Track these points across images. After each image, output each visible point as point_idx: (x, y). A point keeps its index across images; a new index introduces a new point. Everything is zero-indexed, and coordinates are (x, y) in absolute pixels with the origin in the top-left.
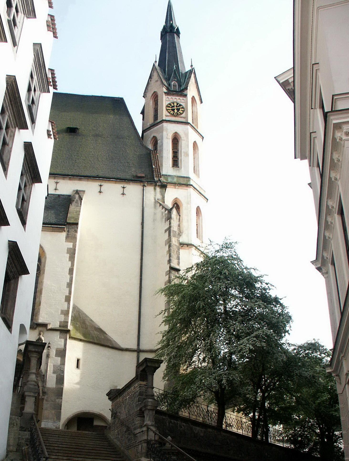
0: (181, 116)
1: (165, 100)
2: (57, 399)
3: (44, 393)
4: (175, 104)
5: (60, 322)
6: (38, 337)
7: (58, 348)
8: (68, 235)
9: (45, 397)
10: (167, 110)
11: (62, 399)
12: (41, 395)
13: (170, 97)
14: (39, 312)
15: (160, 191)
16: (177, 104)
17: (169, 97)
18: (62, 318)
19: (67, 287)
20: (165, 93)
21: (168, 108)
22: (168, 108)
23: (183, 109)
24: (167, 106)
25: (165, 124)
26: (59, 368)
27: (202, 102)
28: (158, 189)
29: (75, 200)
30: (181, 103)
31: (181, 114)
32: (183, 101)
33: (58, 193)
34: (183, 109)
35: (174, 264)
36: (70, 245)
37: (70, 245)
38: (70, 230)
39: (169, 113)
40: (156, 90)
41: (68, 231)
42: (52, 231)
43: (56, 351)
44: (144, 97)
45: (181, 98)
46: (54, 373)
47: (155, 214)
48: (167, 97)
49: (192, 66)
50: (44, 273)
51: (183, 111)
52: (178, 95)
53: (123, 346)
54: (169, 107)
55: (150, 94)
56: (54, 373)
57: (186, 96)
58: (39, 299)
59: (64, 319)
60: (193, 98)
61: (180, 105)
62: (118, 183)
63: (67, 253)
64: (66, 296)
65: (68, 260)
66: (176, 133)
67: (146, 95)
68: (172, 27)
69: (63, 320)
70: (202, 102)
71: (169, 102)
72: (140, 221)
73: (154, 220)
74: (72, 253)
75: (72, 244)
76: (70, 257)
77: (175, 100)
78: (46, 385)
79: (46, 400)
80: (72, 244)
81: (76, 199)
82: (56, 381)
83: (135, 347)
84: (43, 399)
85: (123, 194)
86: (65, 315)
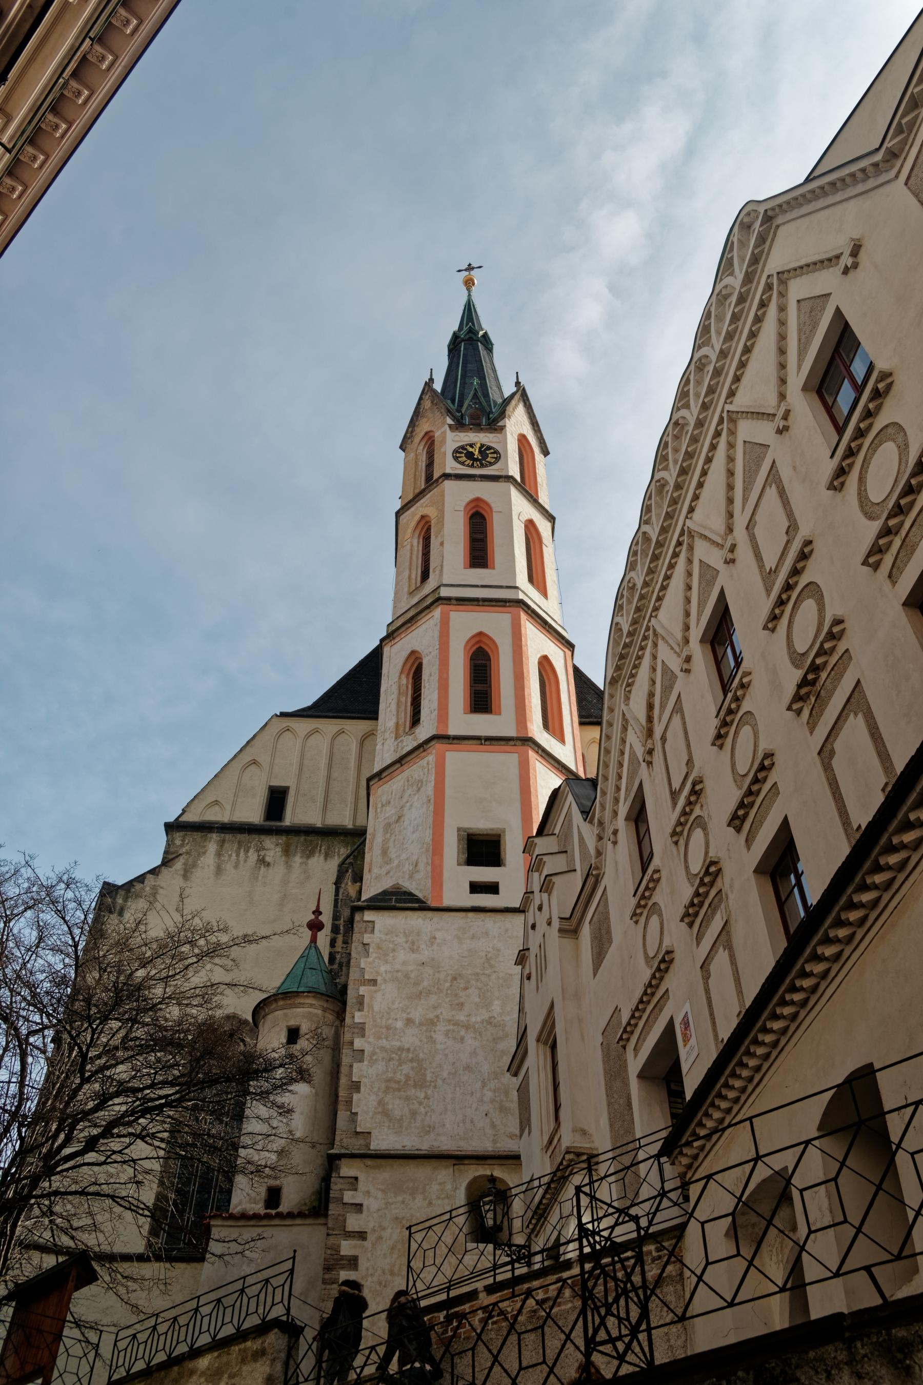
1: (451, 440)
10: (456, 459)
13: (462, 435)
20: (450, 426)
24: (456, 451)
25: (448, 484)
27: (546, 452)
31: (491, 464)
34: (495, 455)
39: (463, 463)
44: (401, 447)
51: (498, 459)
54: (461, 453)
57: (503, 428)
60: (522, 439)
61: (489, 448)
66: (478, 500)
68: (472, 332)
70: (546, 452)
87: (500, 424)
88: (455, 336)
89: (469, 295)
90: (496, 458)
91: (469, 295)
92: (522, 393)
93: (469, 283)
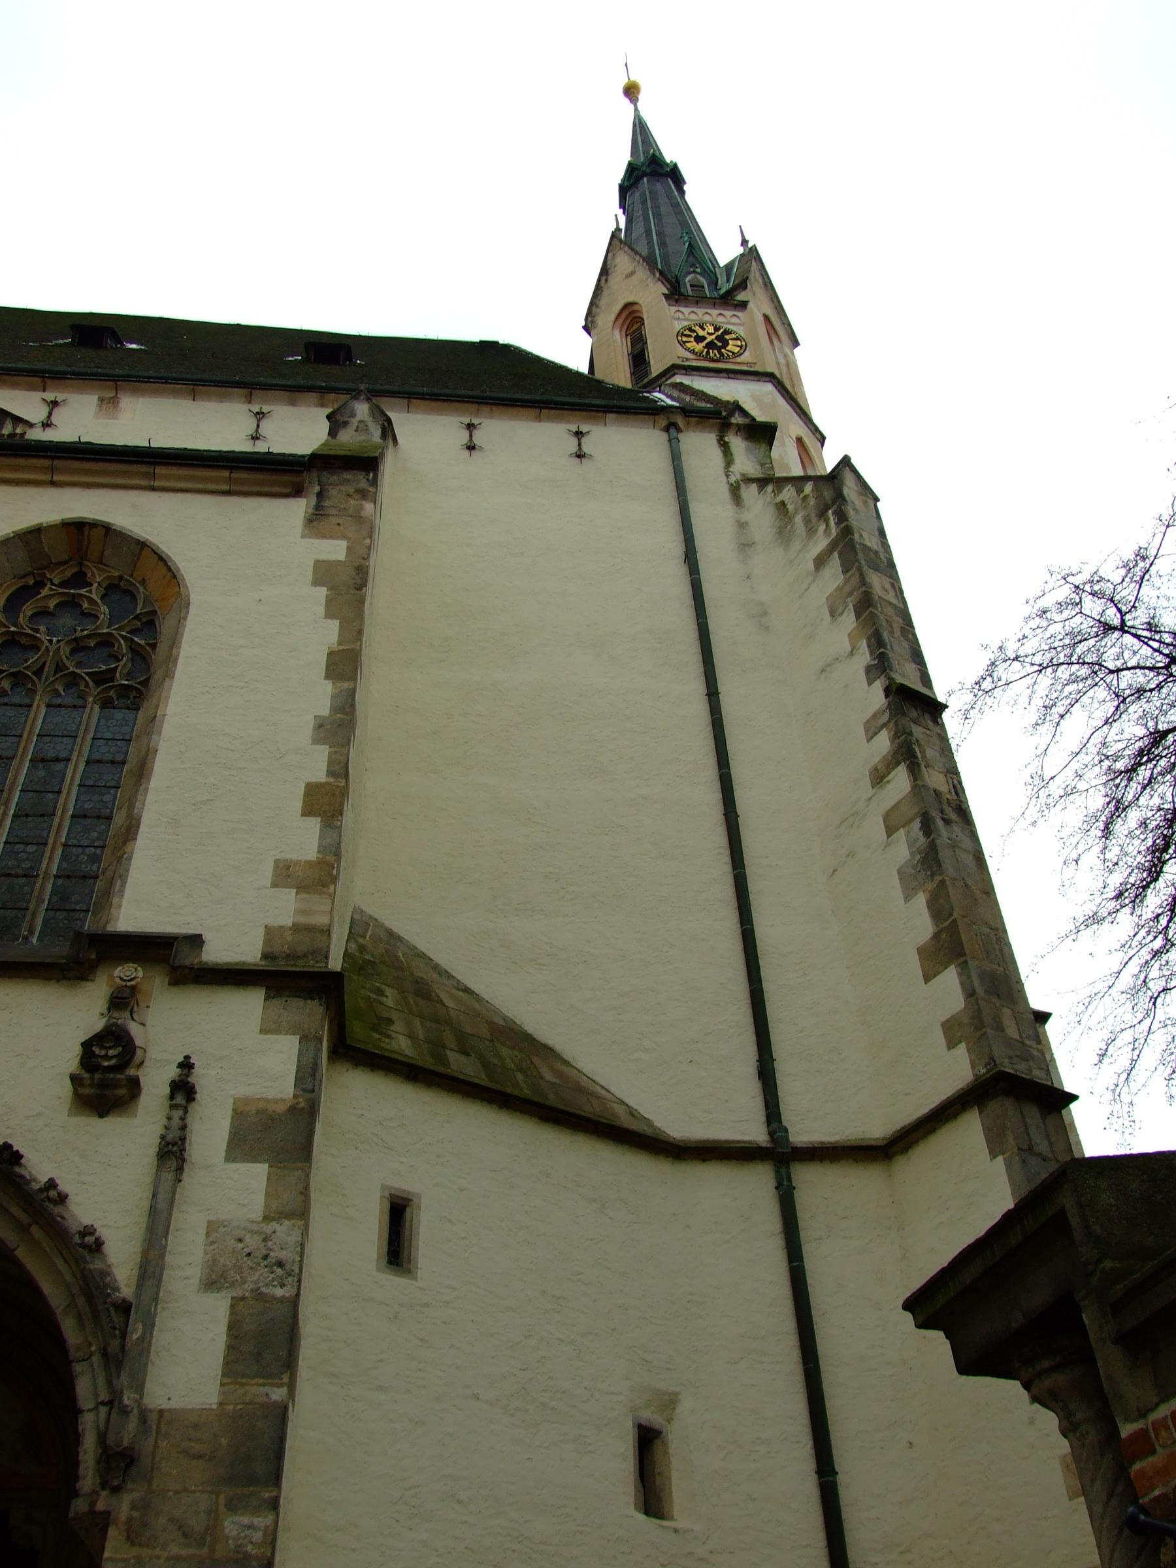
0: (739, 360)
2: (233, 1507)
3: (120, 1463)
4: (711, 330)
5: (269, 930)
6: (99, 1025)
7: (247, 1101)
8: (318, 507)
9: (123, 1506)
11: (274, 1505)
12: (88, 1479)
13: (686, 310)
14: (124, 879)
15: (747, 449)
16: (717, 329)
17: (682, 309)
18: (285, 908)
19: (316, 741)
21: (684, 339)
22: (684, 339)
23: (739, 343)
26: (252, 1242)
28: (737, 443)
29: (354, 422)
30: (729, 327)
32: (734, 320)
33: (261, 447)
34: (739, 343)
35: (907, 676)
36: (335, 550)
37: (335, 550)
38: (333, 492)
40: (630, 299)
41: (320, 495)
42: (228, 493)
43: (238, 1114)
45: (728, 313)
46: (212, 1283)
47: (742, 525)
48: (673, 309)
49: (744, 242)
50: (169, 675)
51: (743, 348)
52: (714, 306)
53: (678, 1128)
55: (606, 318)
56: (212, 1283)
57: (743, 305)
58: (131, 807)
59: (298, 912)
61: (727, 332)
62: (550, 419)
63: (316, 582)
64: (312, 791)
65: (321, 610)
67: (592, 322)
69: (288, 921)
71: (686, 323)
72: (678, 549)
73: (745, 546)
74: (348, 590)
75: (344, 544)
76: (329, 602)
77: (707, 318)
78: (140, 1388)
79: (132, 1537)
80: (344, 544)
81: (358, 418)
82: (230, 1348)
83: (752, 1129)
84: (102, 1521)
85: (580, 456)
86: (301, 888)
87: (741, 297)
88: (631, 169)
89: (636, 109)
90: (741, 347)
91: (636, 109)
92: (751, 255)
93: (631, 91)
